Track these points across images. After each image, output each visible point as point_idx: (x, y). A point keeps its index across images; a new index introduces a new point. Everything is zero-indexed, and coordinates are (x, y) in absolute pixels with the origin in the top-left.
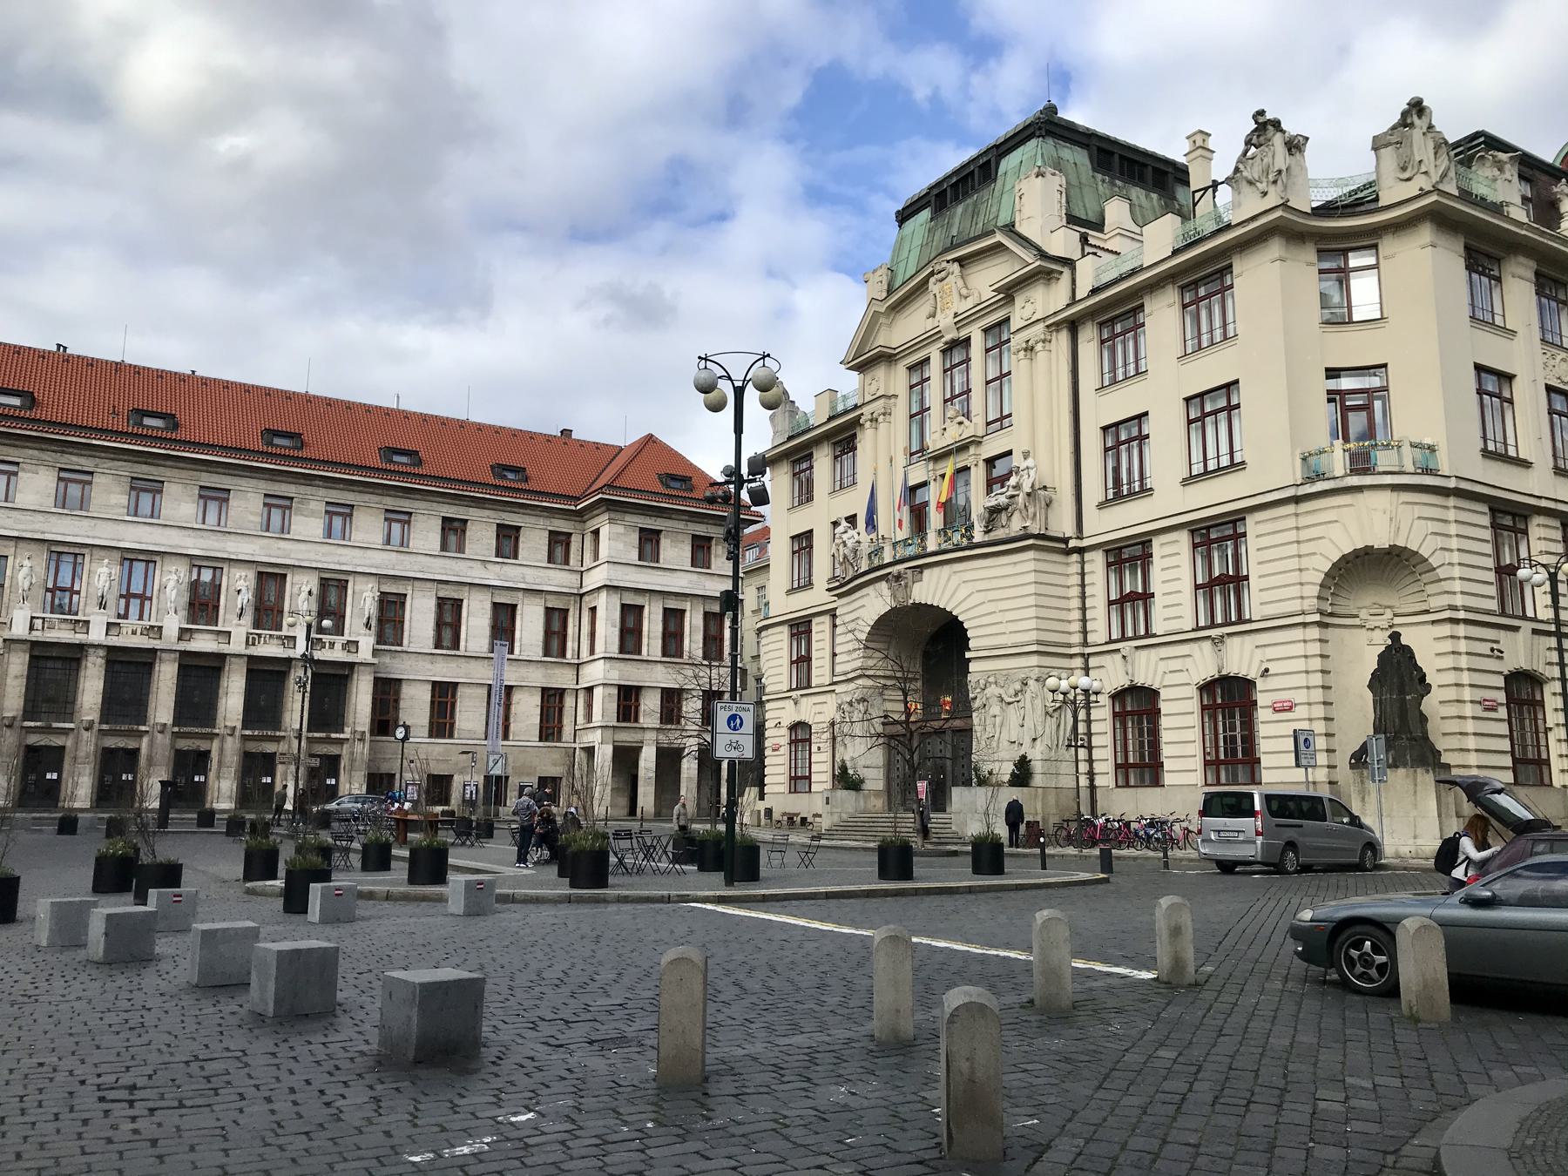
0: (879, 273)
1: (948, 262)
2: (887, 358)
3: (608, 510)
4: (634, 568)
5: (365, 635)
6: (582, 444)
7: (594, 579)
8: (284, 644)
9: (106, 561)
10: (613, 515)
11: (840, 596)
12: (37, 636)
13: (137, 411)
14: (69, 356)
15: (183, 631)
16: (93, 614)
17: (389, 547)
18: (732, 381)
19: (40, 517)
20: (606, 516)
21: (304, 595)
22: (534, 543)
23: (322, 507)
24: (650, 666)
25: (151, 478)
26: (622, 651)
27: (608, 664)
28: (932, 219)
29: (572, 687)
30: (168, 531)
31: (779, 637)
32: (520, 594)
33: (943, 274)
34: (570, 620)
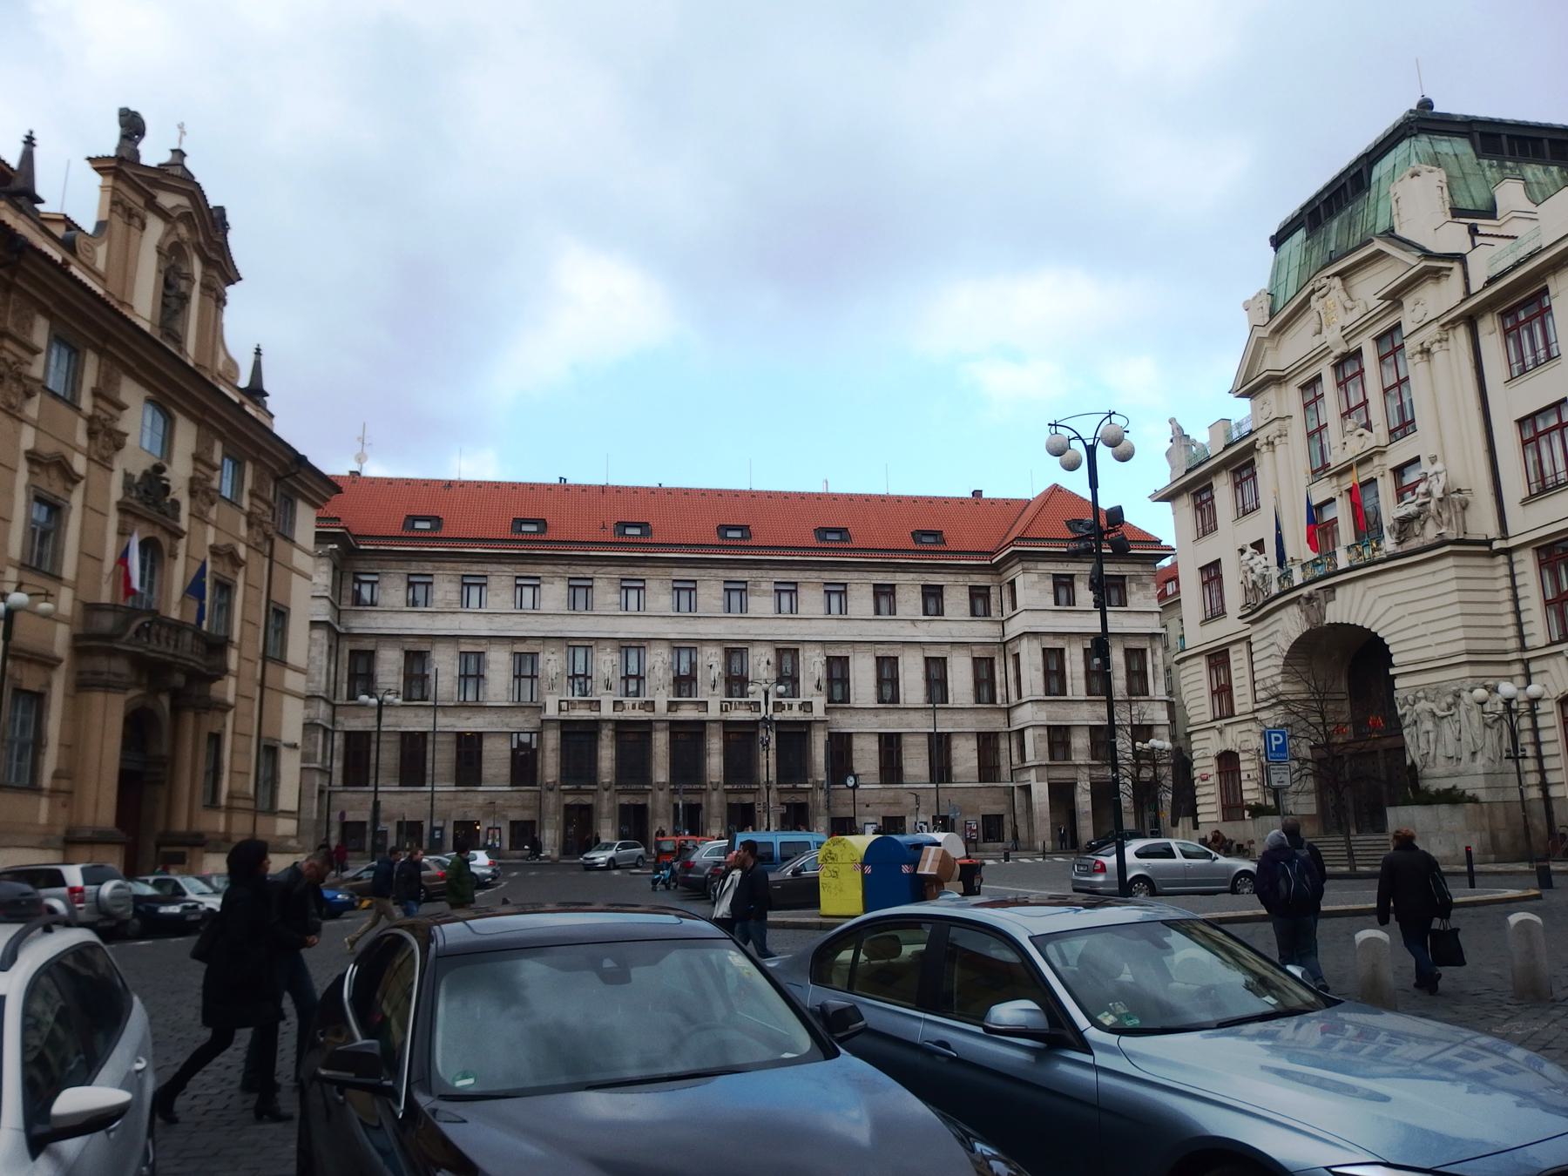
0: (1258, 300)
1: (1328, 277)
2: (1277, 380)
3: (1021, 561)
4: (1050, 613)
6: (993, 502)
7: (1013, 628)
9: (608, 650)
10: (1026, 565)
11: (1253, 622)
12: (564, 716)
13: (619, 523)
14: (569, 485)
15: (671, 704)
16: (603, 694)
17: (830, 616)
18: (1083, 441)
19: (558, 619)
20: (1019, 567)
21: (764, 664)
22: (956, 599)
23: (771, 587)
24: (1076, 706)
25: (635, 577)
26: (1048, 693)
27: (1035, 707)
28: (1307, 239)
29: (1004, 730)
30: (651, 620)
31: (1198, 669)
32: (948, 647)
33: (1324, 291)
34: (997, 668)
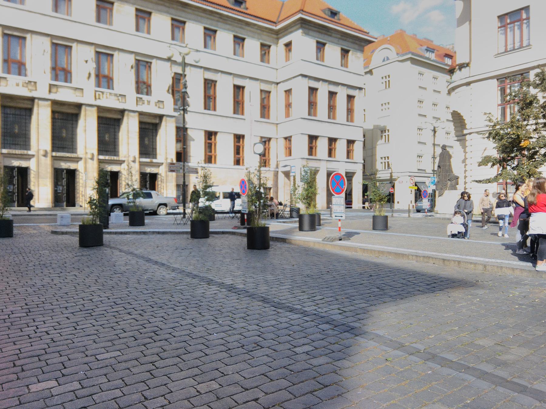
8: (119, 100)
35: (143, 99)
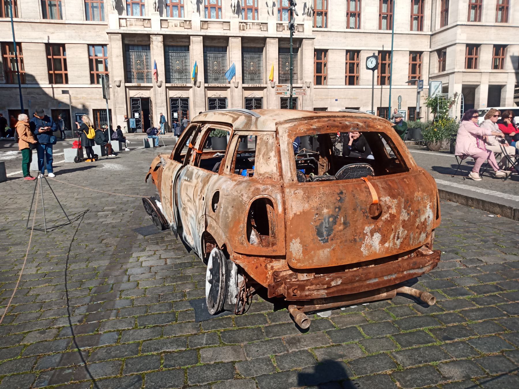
5: (307, 20)
8: (261, 28)
12: (124, 30)
35: (284, 25)
